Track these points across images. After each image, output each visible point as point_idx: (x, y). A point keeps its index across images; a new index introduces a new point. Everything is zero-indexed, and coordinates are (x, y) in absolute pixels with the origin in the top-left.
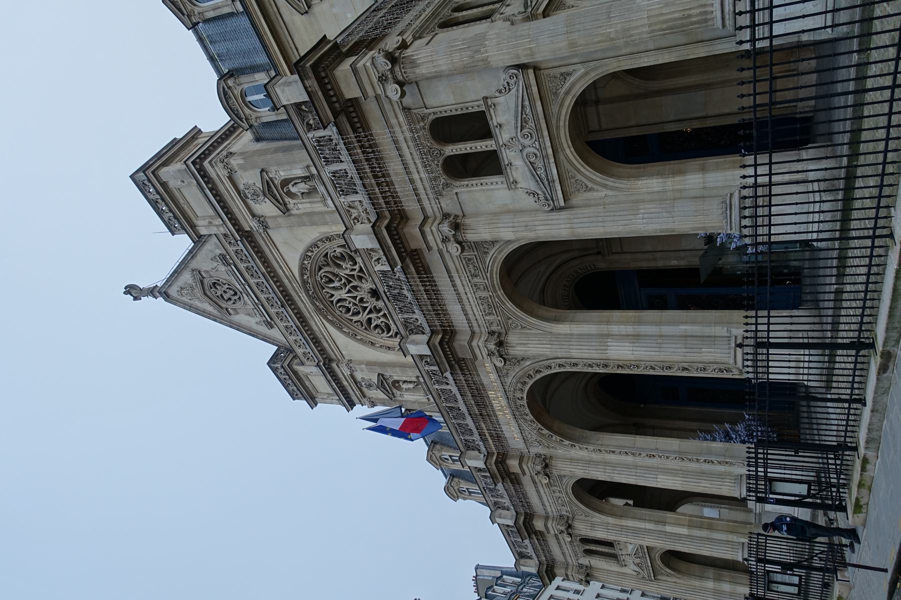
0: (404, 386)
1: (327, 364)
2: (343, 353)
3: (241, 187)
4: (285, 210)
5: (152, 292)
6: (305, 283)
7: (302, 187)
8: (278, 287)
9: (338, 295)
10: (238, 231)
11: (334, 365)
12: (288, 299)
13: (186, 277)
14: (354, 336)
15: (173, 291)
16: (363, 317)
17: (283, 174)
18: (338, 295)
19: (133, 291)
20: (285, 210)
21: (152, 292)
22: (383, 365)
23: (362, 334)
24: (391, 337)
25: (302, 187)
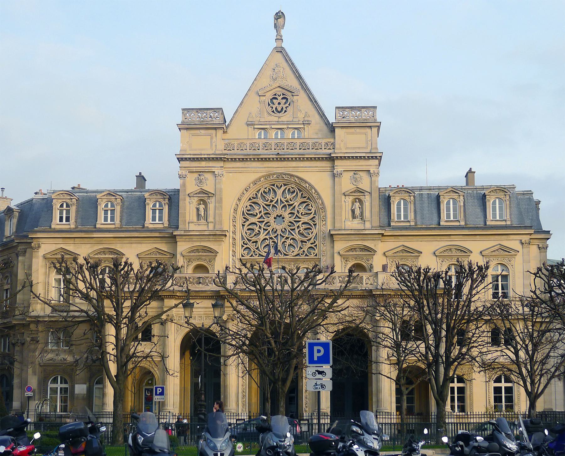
0: (202, 207)
2: (231, 174)
3: (361, 173)
5: (279, 39)
6: (292, 176)
8: (292, 158)
9: (279, 192)
10: (337, 157)
11: (221, 164)
13: (293, 83)
16: (260, 201)
17: (367, 205)
18: (279, 192)
21: (279, 39)
22: (220, 201)
23: (248, 195)
24: (243, 214)
25: (357, 212)
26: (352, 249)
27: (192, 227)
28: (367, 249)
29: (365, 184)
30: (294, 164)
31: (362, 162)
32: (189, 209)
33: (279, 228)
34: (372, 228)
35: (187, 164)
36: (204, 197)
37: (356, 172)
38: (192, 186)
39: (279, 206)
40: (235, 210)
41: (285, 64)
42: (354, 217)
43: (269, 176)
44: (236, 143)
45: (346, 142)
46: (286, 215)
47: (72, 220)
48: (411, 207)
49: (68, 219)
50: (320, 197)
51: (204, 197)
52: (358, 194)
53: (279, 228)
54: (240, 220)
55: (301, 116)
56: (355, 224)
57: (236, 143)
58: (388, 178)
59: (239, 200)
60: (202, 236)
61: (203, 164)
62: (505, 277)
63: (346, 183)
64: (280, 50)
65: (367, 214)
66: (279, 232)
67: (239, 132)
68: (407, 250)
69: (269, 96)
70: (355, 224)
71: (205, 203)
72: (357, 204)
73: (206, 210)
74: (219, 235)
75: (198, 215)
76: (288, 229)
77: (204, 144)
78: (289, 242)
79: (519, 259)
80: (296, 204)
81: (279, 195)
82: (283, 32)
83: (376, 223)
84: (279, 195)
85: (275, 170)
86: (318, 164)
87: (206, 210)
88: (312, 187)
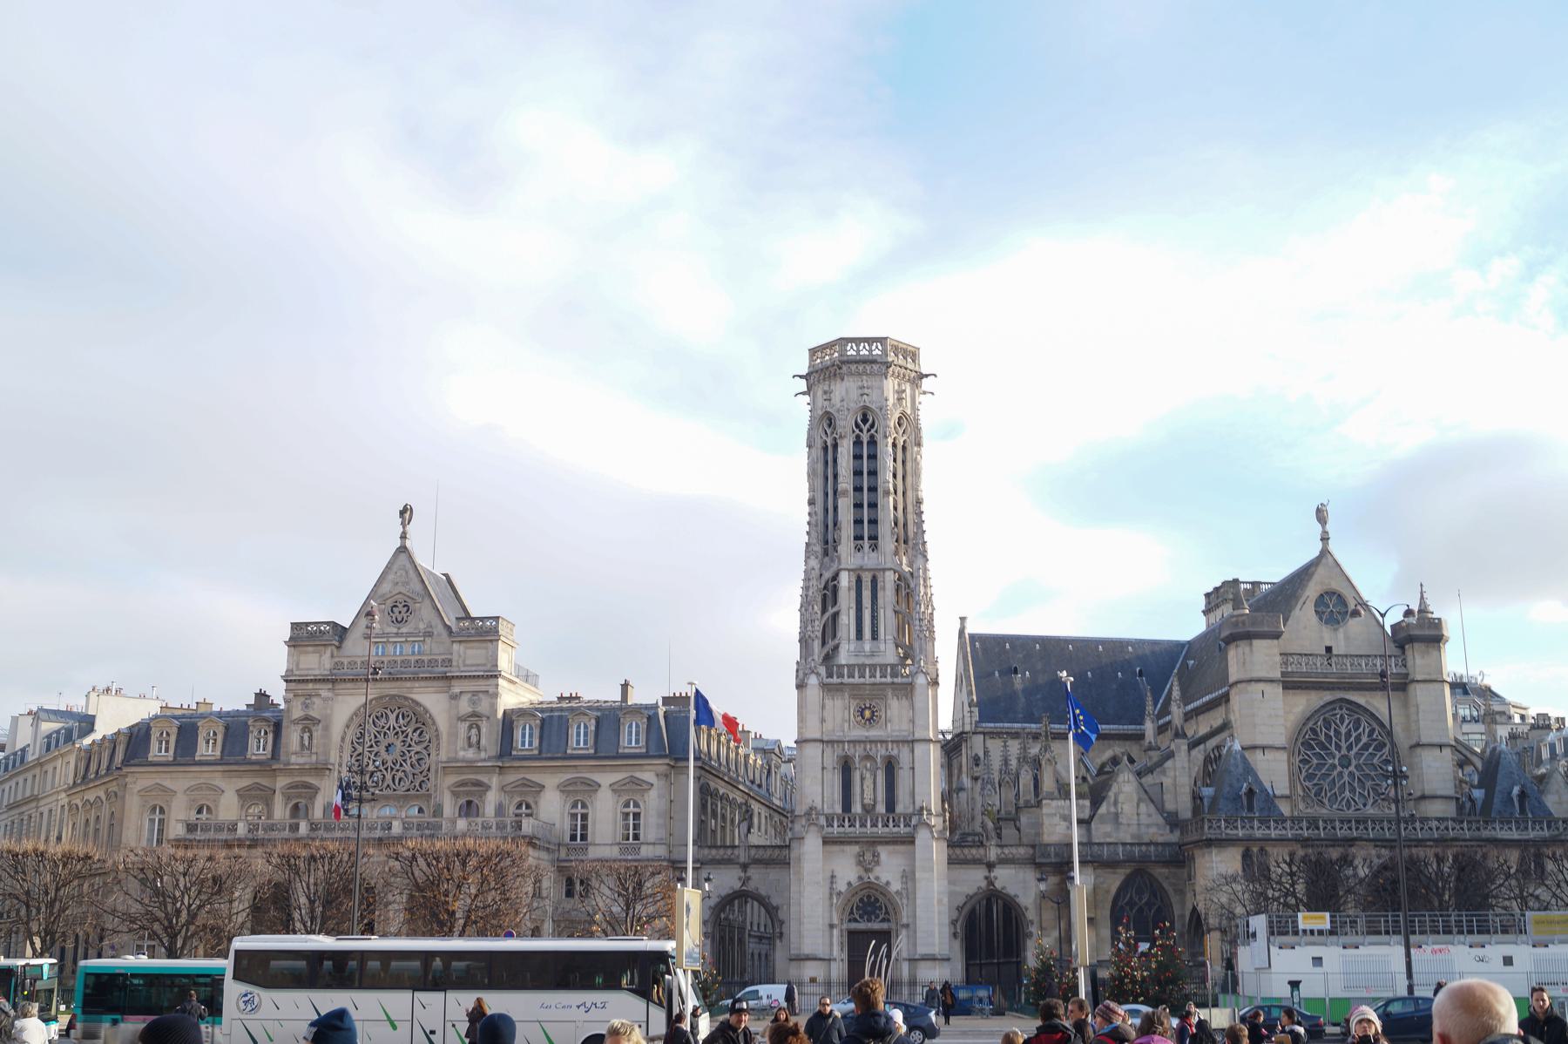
0: (306, 736)
1: (332, 680)
4: (461, 719)
5: (404, 536)
6: (406, 698)
7: (474, 739)
9: (392, 717)
12: (393, 679)
13: (418, 587)
14: (355, 714)
15: (403, 557)
17: (484, 730)
18: (392, 717)
19: (406, 513)
20: (461, 719)
21: (404, 536)
22: (327, 728)
23: (357, 721)
25: (474, 739)
26: (463, 784)
27: (293, 759)
28: (478, 784)
29: (483, 707)
30: (408, 684)
31: (481, 682)
32: (292, 737)
33: (389, 758)
34: (489, 759)
35: (293, 686)
36: (308, 723)
37: (475, 693)
38: (297, 713)
39: (391, 733)
40: (343, 739)
41: (408, 566)
42: (470, 745)
43: (381, 698)
44: (346, 661)
45: (467, 656)
46: (398, 744)
47: (171, 752)
48: (536, 733)
49: (167, 750)
50: (434, 723)
51: (308, 723)
52: (474, 719)
53: (389, 758)
54: (348, 749)
55: (422, 626)
56: (470, 754)
57: (346, 661)
58: (510, 697)
59: (348, 727)
60: (302, 770)
61: (310, 686)
62: (637, 816)
63: (464, 706)
64: (403, 549)
65: (483, 742)
66: (390, 764)
67: (356, 648)
68: (527, 784)
69: (390, 603)
70: (470, 754)
71: (310, 731)
72: (474, 731)
73: (311, 738)
74: (321, 769)
75: (302, 745)
76: (390, 764)
77: (317, 662)
78: (400, 774)
79: (653, 794)
80: (410, 730)
81: (392, 722)
82: (408, 528)
83: (493, 750)
84: (392, 722)
85: (387, 692)
86: (435, 683)
87: (311, 738)
88: (427, 711)
